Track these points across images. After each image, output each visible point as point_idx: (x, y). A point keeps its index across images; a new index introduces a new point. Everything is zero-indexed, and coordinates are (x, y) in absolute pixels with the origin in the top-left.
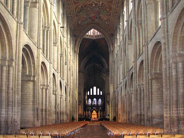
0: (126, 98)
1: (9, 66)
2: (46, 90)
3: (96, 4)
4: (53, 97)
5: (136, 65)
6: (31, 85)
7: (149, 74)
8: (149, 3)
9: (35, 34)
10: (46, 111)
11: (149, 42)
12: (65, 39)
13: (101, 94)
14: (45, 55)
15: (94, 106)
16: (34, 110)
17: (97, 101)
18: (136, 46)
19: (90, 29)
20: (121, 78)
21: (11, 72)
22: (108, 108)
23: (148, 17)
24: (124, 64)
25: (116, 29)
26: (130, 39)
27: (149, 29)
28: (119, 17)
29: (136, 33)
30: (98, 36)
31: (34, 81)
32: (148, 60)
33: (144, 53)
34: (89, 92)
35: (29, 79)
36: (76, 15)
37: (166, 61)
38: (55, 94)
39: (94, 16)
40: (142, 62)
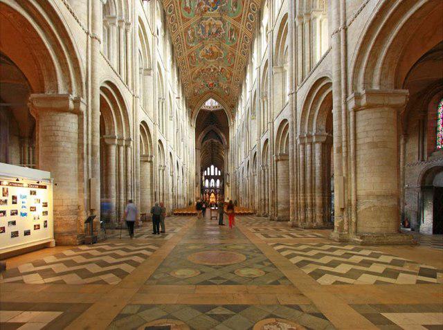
1: (126, 147)
2: (163, 170)
3: (215, 69)
4: (170, 178)
6: (148, 165)
8: (276, 73)
9: (150, 108)
10: (163, 194)
12: (181, 111)
14: (161, 132)
15: (212, 188)
16: (152, 194)
17: (215, 182)
19: (207, 100)
21: (129, 152)
22: (227, 190)
26: (253, 113)
27: (275, 103)
28: (241, 86)
31: (151, 162)
33: (269, 131)
35: (146, 159)
38: (172, 176)
40: (267, 140)
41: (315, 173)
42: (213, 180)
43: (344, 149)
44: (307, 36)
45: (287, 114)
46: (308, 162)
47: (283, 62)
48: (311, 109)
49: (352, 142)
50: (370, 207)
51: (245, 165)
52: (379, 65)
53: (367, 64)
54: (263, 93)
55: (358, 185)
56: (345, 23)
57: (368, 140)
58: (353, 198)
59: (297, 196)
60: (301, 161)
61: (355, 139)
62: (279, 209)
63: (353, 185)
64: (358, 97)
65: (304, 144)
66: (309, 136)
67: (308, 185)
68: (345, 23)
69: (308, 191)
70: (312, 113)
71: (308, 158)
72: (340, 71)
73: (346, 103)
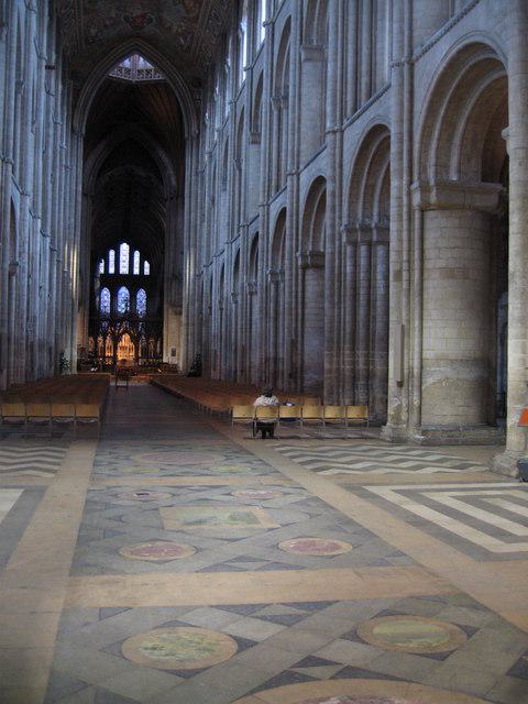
0: (236, 302)
5: (268, 214)
7: (299, 253)
8: (307, 60)
11: (301, 167)
13: (147, 271)
18: (270, 161)
20: (224, 236)
23: (303, 98)
24: (234, 195)
25: (213, 67)
28: (224, 37)
29: (271, 120)
30: (148, 71)
32: (298, 215)
34: (102, 265)
36: (85, 9)
37: (333, 235)
39: (143, 16)
40: (283, 212)
41: (375, 307)
42: (124, 292)
43: (405, 274)
44: (365, 18)
45: (323, 166)
46: (363, 283)
47: (323, 37)
48: (368, 173)
49: (416, 264)
50: (440, 382)
51: (227, 258)
52: (457, 140)
53: (440, 135)
54: (278, 89)
55: (425, 341)
56: (411, 53)
57: (441, 263)
58: (416, 363)
59: (338, 356)
60: (348, 278)
61: (422, 260)
62: (307, 383)
63: (417, 341)
64: (424, 188)
65: (355, 245)
66: (366, 229)
67: (361, 332)
68: (411, 53)
69: (361, 345)
70: (371, 182)
71: (362, 275)
72: (401, 133)
73: (409, 194)
